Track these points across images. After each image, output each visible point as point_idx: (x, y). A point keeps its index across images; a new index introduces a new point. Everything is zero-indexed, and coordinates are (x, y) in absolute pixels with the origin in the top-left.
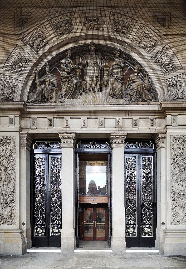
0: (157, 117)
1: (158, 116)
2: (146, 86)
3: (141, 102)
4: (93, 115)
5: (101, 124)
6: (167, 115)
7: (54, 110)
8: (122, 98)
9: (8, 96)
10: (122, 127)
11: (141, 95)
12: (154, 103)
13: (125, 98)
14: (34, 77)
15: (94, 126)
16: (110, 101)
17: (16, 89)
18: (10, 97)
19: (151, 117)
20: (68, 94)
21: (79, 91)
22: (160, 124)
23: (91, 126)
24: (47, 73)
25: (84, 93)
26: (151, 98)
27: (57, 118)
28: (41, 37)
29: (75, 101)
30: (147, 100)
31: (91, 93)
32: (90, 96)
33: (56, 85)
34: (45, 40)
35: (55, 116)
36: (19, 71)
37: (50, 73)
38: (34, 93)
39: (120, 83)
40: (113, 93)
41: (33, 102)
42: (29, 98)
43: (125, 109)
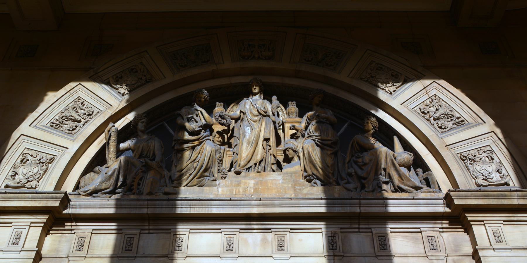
0: (443, 228)
1: (444, 226)
2: (399, 158)
3: (393, 192)
4: (255, 225)
5: (281, 247)
6: (472, 223)
7: (145, 211)
8: (338, 184)
9: (24, 181)
10: (342, 254)
11: (390, 177)
12: (429, 195)
13: (346, 183)
14: (104, 141)
15: (258, 251)
16: (305, 191)
17: (50, 165)
18: (29, 181)
19: (426, 226)
20: (189, 177)
21: (218, 170)
22: (457, 247)
23: (250, 252)
24: (140, 133)
25: (232, 174)
26: (418, 184)
27: (151, 231)
28: (137, 72)
29: (207, 192)
30: (407, 187)
31: (252, 174)
32: (249, 183)
33: (158, 158)
34: (145, 76)
35: (147, 227)
36: (69, 130)
37: (148, 133)
38: (98, 173)
39: (329, 152)
40: (313, 174)
41: (90, 194)
42: (82, 184)
43: (348, 209)
